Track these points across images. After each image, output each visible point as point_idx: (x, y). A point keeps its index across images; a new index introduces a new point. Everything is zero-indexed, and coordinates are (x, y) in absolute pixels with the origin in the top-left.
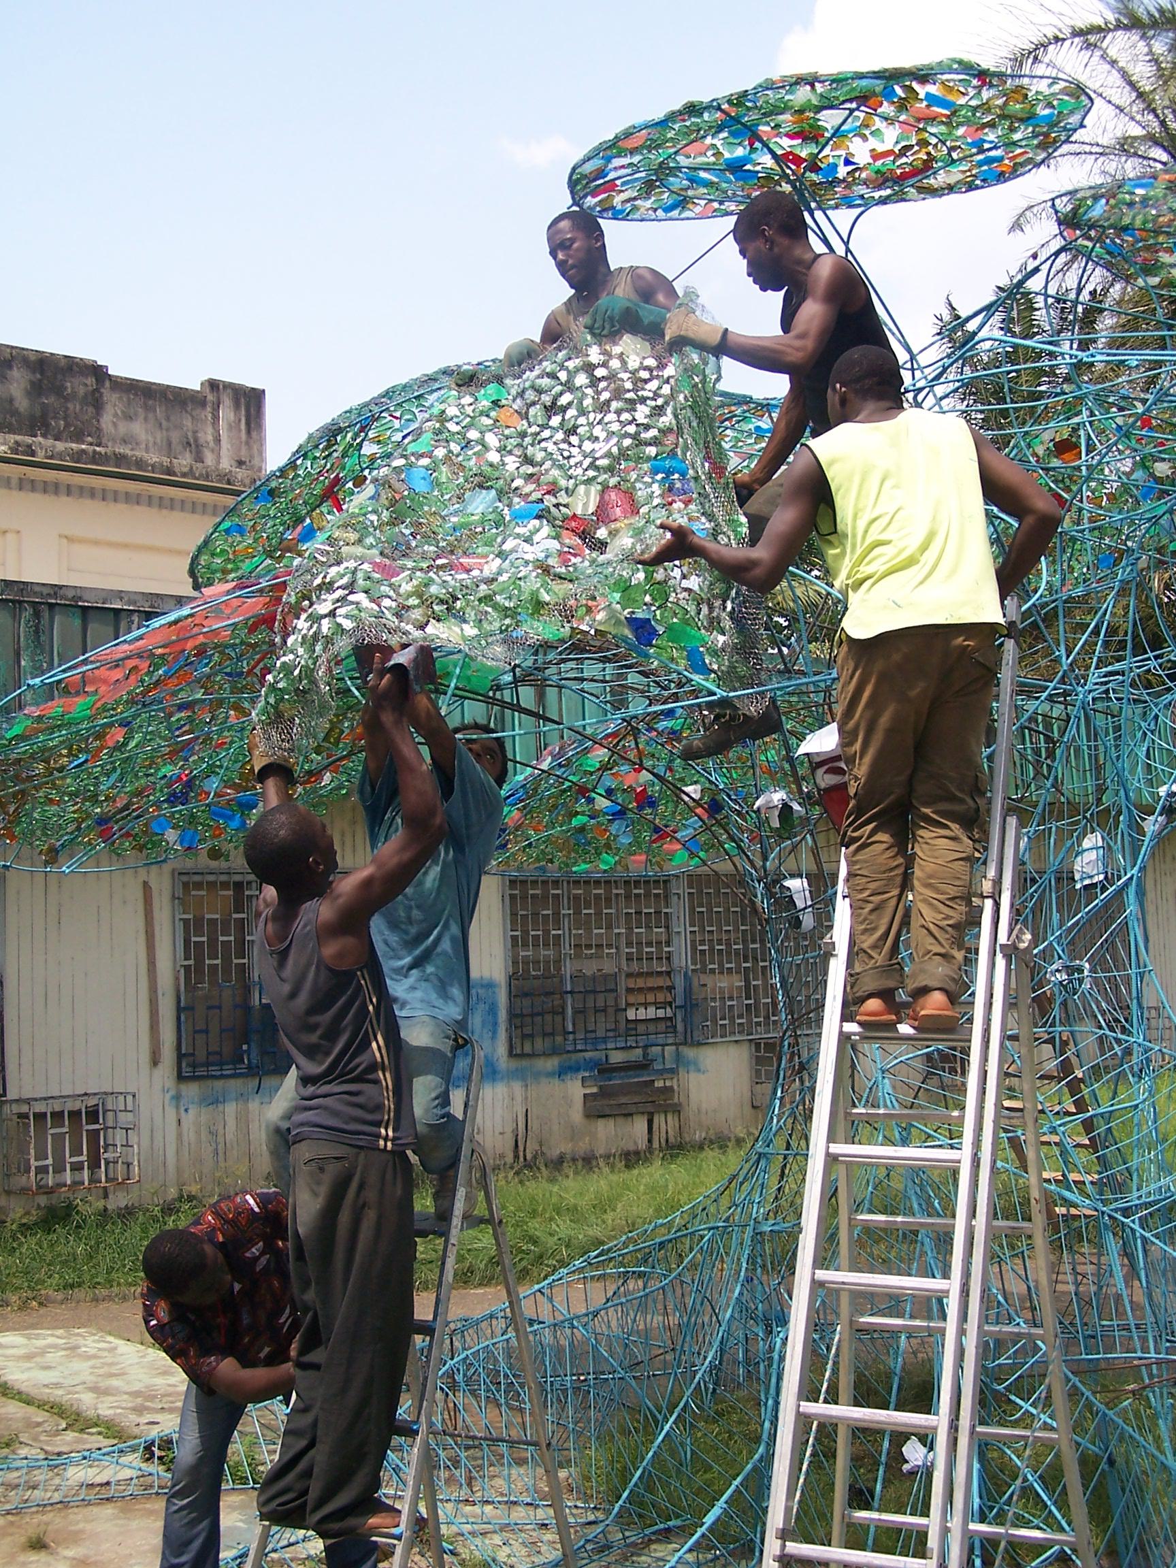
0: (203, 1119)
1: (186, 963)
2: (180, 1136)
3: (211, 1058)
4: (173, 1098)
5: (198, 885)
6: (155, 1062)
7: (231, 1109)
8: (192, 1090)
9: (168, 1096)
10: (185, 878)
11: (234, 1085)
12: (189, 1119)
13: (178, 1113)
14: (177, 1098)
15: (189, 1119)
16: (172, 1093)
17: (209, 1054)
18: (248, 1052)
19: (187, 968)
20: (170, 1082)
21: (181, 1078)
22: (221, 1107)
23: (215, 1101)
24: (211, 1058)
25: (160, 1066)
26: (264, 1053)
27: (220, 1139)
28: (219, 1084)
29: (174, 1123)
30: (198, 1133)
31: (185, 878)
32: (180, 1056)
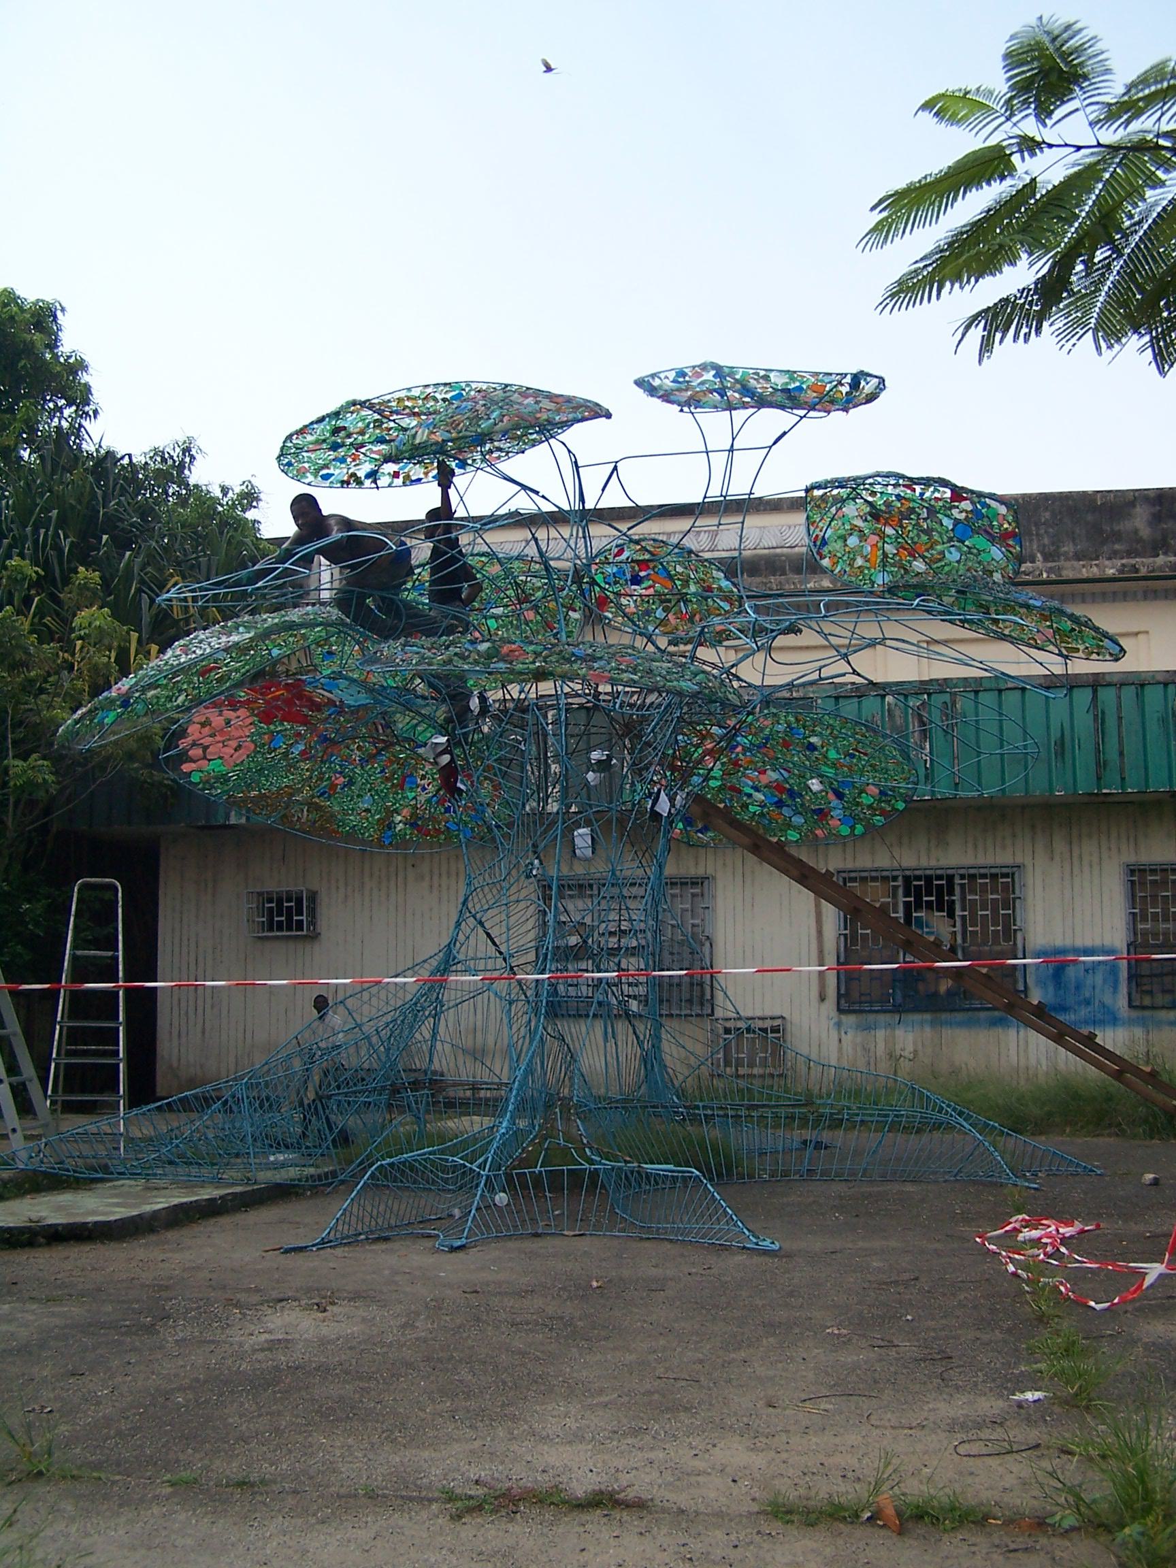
0: (859, 1040)
1: (844, 932)
2: (840, 1050)
3: (863, 998)
4: (835, 1024)
5: (853, 880)
6: (822, 998)
7: (881, 1034)
8: (850, 1019)
9: (832, 1022)
10: (844, 875)
11: (882, 1018)
12: (848, 1039)
13: (839, 1033)
14: (839, 1025)
15: (848, 1039)
16: (835, 1020)
17: (861, 995)
18: (893, 995)
19: (845, 935)
20: (833, 1013)
21: (840, 1010)
22: (873, 1032)
23: (868, 1028)
24: (863, 998)
25: (826, 1002)
26: (904, 997)
27: (872, 1054)
28: (871, 1017)
29: (836, 1042)
30: (855, 1050)
31: (844, 875)
32: (839, 996)
